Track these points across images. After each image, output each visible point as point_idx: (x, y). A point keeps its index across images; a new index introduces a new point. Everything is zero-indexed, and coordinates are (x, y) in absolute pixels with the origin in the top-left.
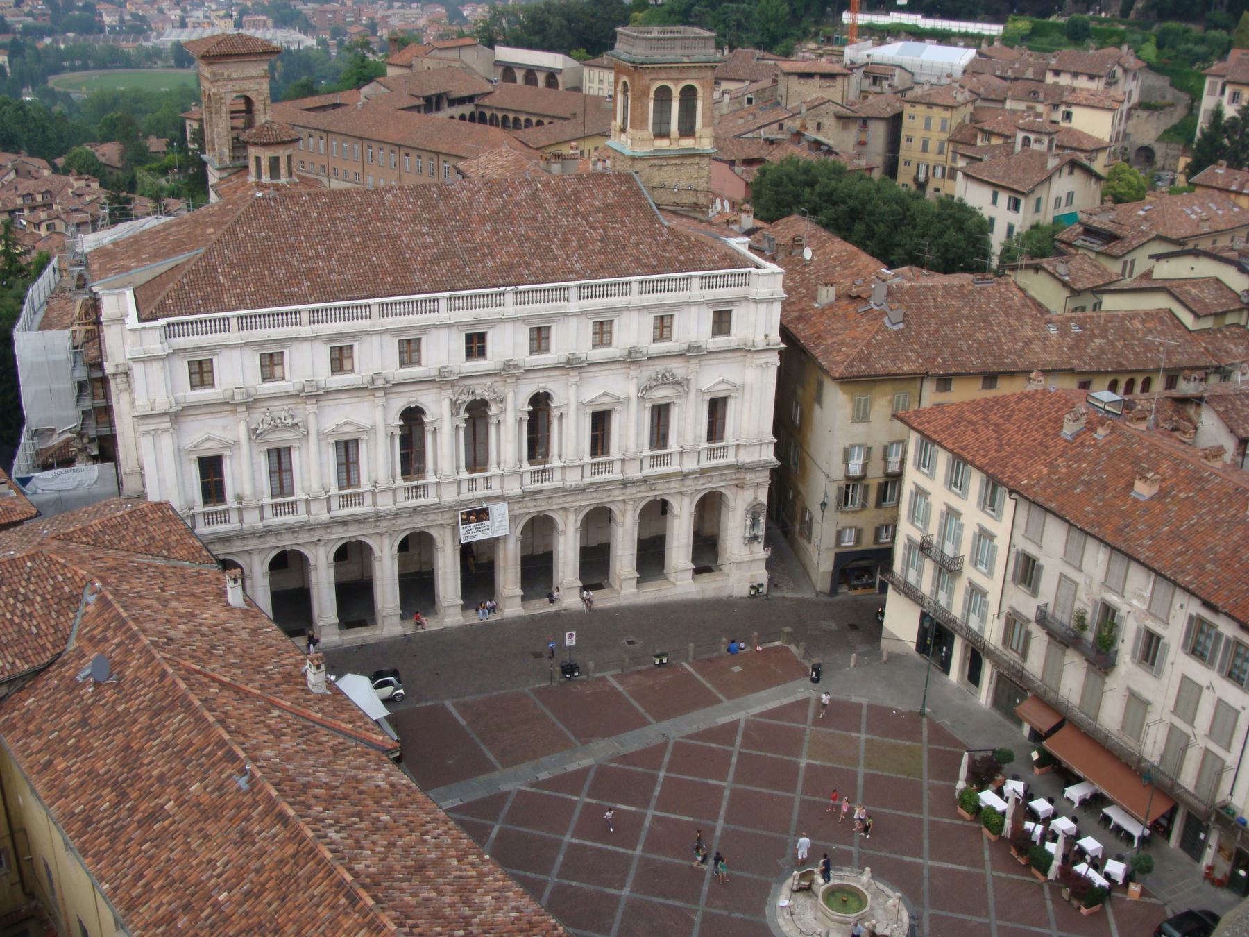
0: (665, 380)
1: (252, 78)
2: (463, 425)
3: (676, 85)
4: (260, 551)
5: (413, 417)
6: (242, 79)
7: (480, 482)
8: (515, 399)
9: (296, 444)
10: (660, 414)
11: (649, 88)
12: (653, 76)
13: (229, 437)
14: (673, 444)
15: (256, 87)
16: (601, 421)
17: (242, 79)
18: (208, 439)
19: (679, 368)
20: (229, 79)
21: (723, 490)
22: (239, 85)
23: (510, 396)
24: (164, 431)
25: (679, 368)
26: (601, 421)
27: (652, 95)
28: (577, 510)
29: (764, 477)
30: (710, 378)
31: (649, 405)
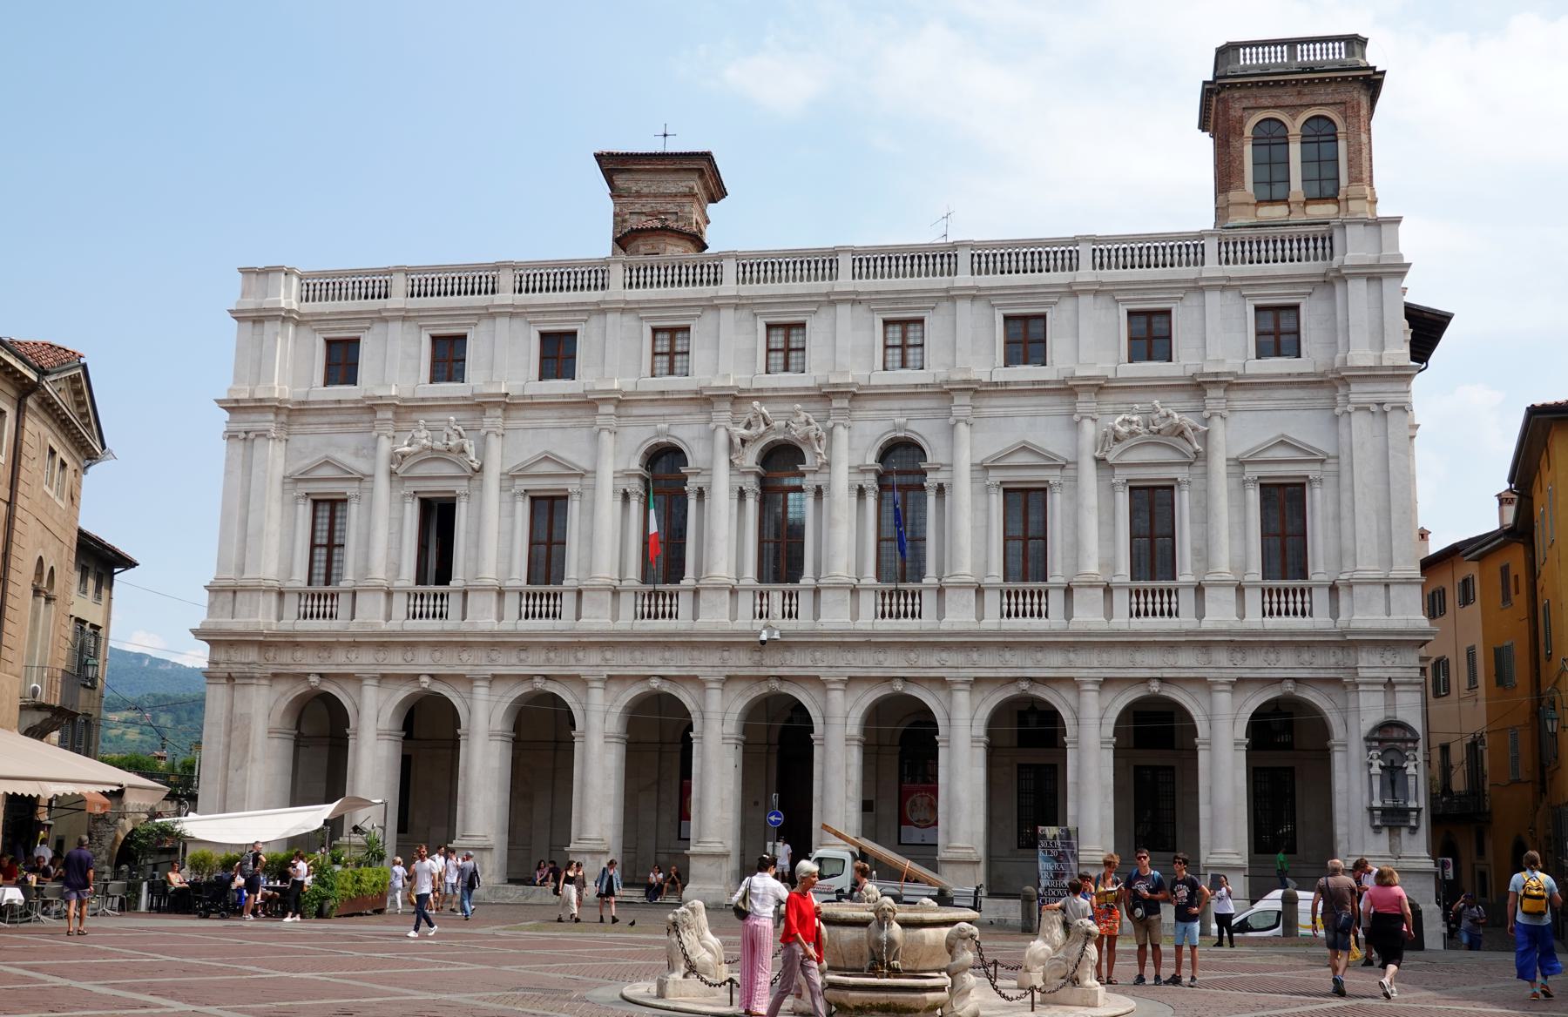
1: (670, 195)
6: (655, 196)
7: (776, 598)
9: (460, 487)
11: (1241, 122)
12: (1246, 103)
13: (362, 466)
14: (1186, 574)
15: (671, 208)
17: (655, 196)
18: (327, 463)
20: (639, 195)
21: (1310, 695)
22: (650, 205)
23: (841, 434)
27: (1248, 131)
29: (1405, 665)
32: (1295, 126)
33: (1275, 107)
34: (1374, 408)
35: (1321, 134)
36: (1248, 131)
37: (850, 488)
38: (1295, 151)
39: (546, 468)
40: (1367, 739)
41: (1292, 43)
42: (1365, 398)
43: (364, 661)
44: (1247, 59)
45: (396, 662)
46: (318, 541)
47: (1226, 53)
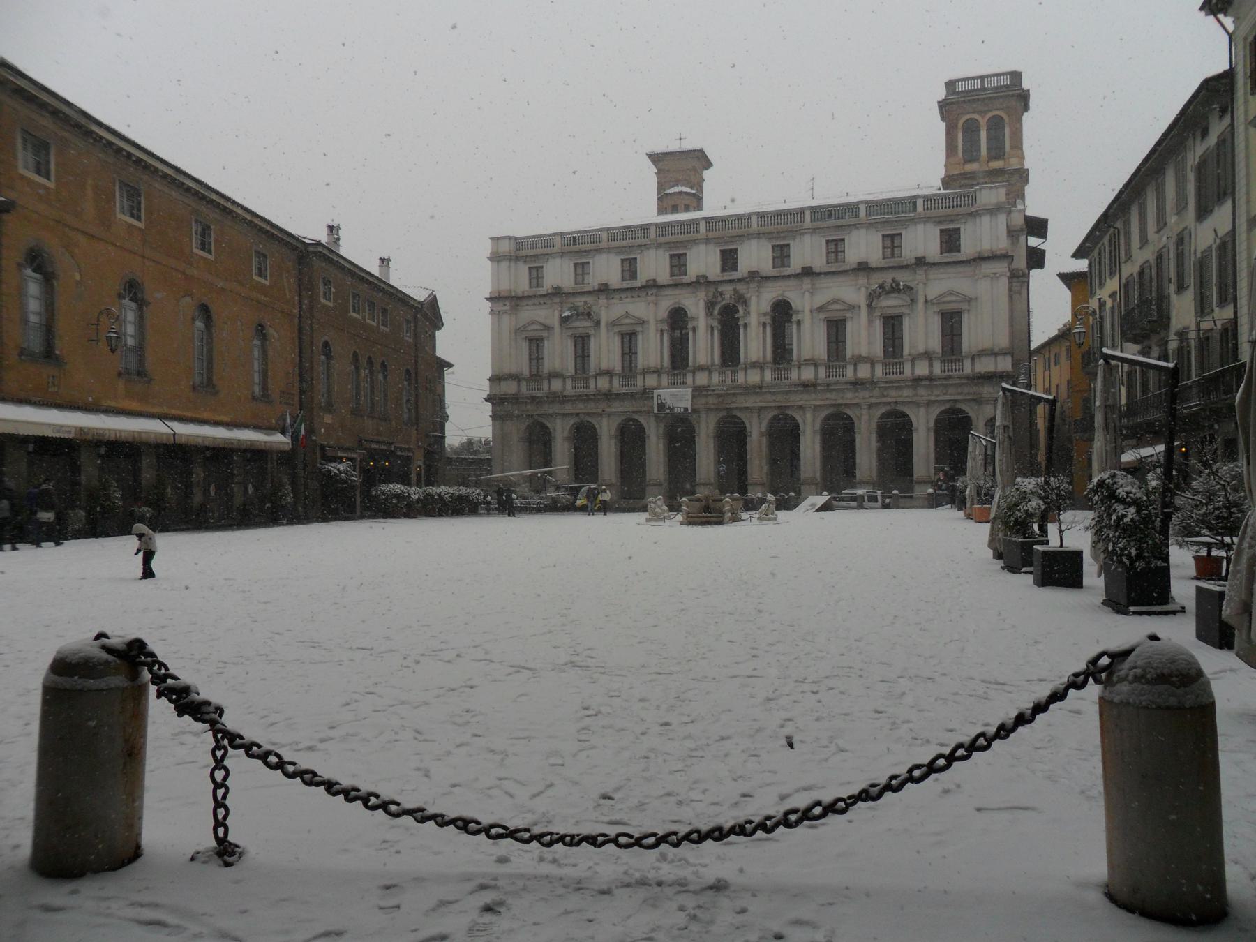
0: (896, 289)
2: (715, 324)
3: (983, 117)
4: (564, 415)
5: (678, 319)
8: (758, 303)
9: (591, 332)
10: (892, 325)
16: (836, 328)
19: (903, 278)
24: (505, 312)
25: (903, 278)
26: (836, 328)
27: (960, 125)
28: (816, 408)
30: (938, 285)
31: (877, 313)
32: (983, 122)
33: (974, 112)
34: (992, 275)
35: (996, 126)
36: (960, 125)
37: (759, 323)
38: (983, 134)
39: (627, 321)
40: (986, 425)
41: (982, 78)
42: (988, 271)
43: (555, 408)
44: (959, 87)
45: (568, 408)
46: (532, 357)
47: (950, 85)
